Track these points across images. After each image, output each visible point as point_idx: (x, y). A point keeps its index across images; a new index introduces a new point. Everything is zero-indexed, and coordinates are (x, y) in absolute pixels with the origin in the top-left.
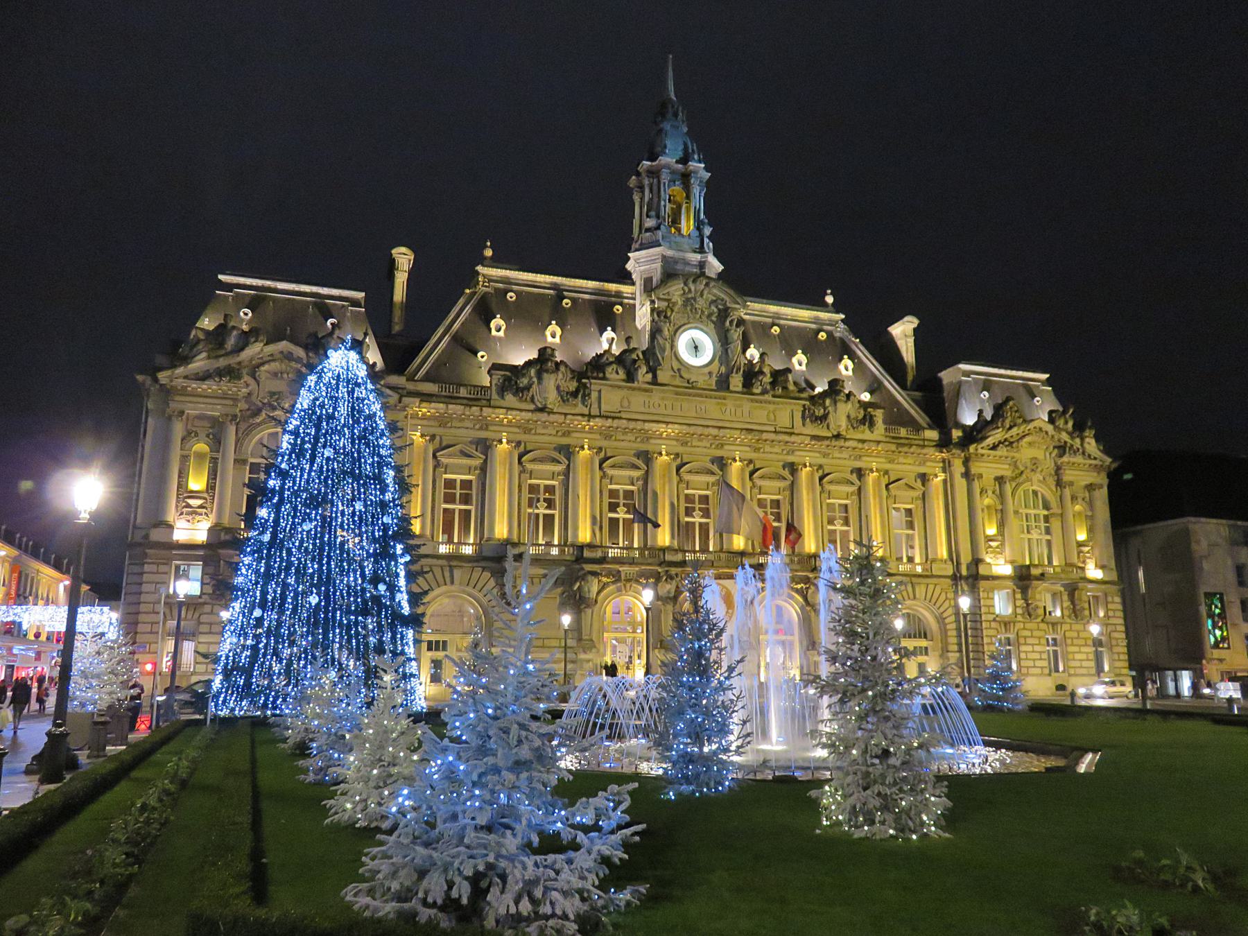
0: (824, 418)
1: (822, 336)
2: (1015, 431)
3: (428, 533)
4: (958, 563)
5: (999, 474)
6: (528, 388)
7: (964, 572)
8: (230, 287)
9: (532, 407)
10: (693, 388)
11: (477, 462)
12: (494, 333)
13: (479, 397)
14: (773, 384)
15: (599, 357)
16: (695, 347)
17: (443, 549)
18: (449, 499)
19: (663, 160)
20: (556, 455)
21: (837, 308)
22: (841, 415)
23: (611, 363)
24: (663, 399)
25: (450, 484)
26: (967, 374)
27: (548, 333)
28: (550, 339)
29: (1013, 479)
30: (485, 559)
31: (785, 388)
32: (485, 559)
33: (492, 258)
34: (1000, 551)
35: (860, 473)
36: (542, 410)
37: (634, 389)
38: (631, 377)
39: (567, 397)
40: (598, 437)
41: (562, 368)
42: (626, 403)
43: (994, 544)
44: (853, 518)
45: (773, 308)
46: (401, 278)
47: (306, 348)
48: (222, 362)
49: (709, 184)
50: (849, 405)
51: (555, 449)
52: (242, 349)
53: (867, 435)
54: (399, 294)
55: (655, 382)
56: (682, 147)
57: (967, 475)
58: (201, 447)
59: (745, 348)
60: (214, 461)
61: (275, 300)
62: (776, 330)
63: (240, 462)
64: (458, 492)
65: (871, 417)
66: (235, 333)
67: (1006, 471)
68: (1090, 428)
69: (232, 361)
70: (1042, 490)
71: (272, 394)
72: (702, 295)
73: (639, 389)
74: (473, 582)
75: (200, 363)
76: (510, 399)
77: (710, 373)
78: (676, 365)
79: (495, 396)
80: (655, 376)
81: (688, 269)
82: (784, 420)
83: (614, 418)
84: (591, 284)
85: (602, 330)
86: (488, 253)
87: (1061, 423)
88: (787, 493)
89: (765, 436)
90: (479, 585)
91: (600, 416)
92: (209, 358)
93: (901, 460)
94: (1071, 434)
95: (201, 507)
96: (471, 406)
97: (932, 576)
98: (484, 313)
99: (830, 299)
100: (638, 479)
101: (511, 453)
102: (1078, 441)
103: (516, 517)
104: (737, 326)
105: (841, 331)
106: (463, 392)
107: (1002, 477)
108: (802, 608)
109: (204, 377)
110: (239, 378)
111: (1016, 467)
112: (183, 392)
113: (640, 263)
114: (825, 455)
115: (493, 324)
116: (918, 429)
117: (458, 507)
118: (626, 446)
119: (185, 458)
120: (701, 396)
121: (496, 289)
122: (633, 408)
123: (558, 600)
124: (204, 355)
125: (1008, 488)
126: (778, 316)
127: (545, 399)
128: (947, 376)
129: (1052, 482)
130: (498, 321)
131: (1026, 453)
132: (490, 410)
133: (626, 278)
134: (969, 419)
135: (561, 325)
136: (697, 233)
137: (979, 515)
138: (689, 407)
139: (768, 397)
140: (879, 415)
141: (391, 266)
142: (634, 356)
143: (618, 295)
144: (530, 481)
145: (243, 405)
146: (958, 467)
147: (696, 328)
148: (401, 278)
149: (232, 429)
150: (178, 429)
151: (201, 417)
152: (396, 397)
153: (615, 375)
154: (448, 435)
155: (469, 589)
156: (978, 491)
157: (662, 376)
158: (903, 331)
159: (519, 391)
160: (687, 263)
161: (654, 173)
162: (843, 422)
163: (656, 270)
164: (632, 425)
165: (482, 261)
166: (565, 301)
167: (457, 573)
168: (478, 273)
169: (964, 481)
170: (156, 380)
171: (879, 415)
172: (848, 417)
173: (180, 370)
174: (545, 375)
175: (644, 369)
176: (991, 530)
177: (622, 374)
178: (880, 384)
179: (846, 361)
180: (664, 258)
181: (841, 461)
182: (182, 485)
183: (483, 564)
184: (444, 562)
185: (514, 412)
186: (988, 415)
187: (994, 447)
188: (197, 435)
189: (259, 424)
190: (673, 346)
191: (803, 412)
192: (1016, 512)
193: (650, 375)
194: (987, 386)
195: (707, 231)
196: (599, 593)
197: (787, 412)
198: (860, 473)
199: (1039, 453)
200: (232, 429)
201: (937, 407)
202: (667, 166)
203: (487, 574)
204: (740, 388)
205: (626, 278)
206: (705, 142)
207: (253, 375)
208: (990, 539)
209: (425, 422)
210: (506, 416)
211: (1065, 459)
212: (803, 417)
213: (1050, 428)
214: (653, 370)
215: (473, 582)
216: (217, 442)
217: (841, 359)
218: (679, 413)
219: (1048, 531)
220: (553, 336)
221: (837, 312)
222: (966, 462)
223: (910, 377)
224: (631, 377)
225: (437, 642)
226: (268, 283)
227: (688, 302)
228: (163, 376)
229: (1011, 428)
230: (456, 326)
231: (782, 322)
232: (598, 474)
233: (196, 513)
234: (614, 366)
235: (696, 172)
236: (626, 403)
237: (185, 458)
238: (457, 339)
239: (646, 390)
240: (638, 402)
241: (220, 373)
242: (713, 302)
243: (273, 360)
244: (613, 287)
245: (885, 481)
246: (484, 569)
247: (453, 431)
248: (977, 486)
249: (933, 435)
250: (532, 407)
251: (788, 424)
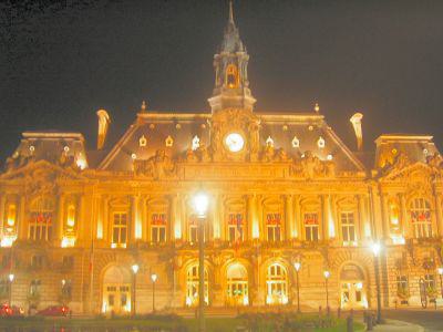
0: (301, 171)
1: (311, 128)
8: (27, 138)
13: (130, 176)
14: (274, 156)
15: (185, 152)
17: (114, 246)
18: (117, 223)
19: (223, 53)
21: (321, 112)
25: (117, 216)
26: (384, 141)
34: (399, 232)
38: (200, 160)
45: (285, 117)
50: (314, 164)
53: (326, 178)
55: (212, 161)
57: (379, 194)
58: (13, 207)
59: (266, 139)
63: (27, 211)
67: (401, 190)
75: (9, 173)
84: (192, 115)
86: (144, 107)
99: (317, 109)
103: (146, 230)
106: (121, 174)
109: (11, 178)
114: (301, 189)
126: (289, 120)
129: (430, 193)
131: (414, 181)
134: (383, 165)
140: (332, 168)
141: (97, 119)
143: (205, 119)
145: (27, 188)
146: (375, 191)
149: (23, 199)
156: (386, 201)
157: (217, 157)
160: (234, 101)
161: (220, 59)
162: (311, 172)
165: (140, 111)
171: (332, 168)
175: (206, 155)
179: (321, 140)
180: (223, 100)
186: (391, 161)
187: (394, 179)
196: (184, 263)
199: (421, 179)
206: (249, 41)
207: (31, 175)
211: (435, 181)
214: (211, 156)
216: (18, 204)
222: (379, 188)
226: (42, 134)
241: (17, 175)
244: (202, 115)
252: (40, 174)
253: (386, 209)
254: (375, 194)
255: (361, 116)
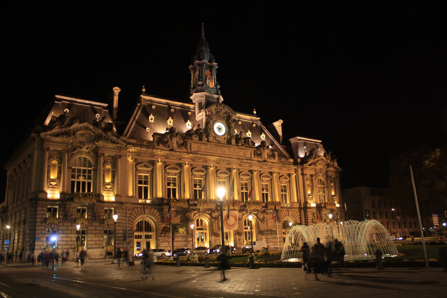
2: (316, 160)
3: (134, 195)
4: (301, 204)
5: (311, 173)
6: (167, 142)
7: (302, 206)
8: (60, 100)
9: (168, 149)
10: (220, 143)
11: (149, 169)
12: (150, 121)
13: (150, 145)
14: (245, 142)
16: (220, 129)
18: (140, 182)
20: (176, 166)
21: (257, 115)
22: (266, 153)
23: (194, 134)
24: (211, 147)
26: (299, 140)
27: (168, 122)
28: (169, 124)
29: (315, 175)
30: (156, 205)
31: (248, 144)
32: (156, 205)
33: (145, 92)
35: (271, 173)
36: (172, 150)
37: (201, 143)
38: (201, 139)
39: (180, 146)
40: (190, 160)
41: (179, 136)
42: (199, 149)
43: (310, 197)
44: (269, 188)
46: (116, 99)
47: (93, 125)
48: (64, 130)
49: (217, 70)
51: (176, 164)
52: (71, 125)
54: (115, 104)
55: (208, 141)
56: (209, 57)
57: (302, 174)
58: (55, 162)
60: (60, 168)
61: (76, 106)
62: (240, 123)
63: (69, 168)
64: (143, 180)
65: (274, 154)
66: (68, 119)
68: (336, 158)
69: (67, 129)
70: (323, 179)
71: (81, 142)
72: (221, 110)
73: (203, 143)
74: (151, 214)
76: (161, 146)
77: (225, 138)
78: (214, 135)
79: (156, 145)
80: (208, 139)
81: (213, 100)
82: (248, 155)
83: (196, 154)
85: (186, 121)
87: (327, 157)
88: (250, 180)
89: (244, 161)
90: (154, 214)
91: (191, 153)
92: (59, 128)
93: (283, 169)
94: (330, 161)
95: (56, 185)
96: (149, 148)
97: (293, 208)
98: (146, 112)
99: (255, 112)
100: (203, 176)
101: (162, 166)
102: (332, 163)
104: (233, 122)
105: (259, 123)
107: (312, 175)
108: (256, 220)
109: (57, 135)
110: (70, 136)
111: (316, 171)
112: (49, 141)
113: (196, 97)
114: (261, 168)
115: (150, 118)
116: (287, 159)
117: (143, 186)
118: (199, 164)
119: (49, 166)
120: (223, 146)
121: (148, 104)
122: (202, 150)
123: (180, 219)
124: (58, 127)
125: (314, 178)
127: (173, 146)
128: (292, 140)
129: (325, 176)
130: (151, 116)
131: (319, 167)
132: (156, 150)
133: (190, 102)
134: (302, 155)
135: (172, 118)
136: (215, 88)
137: (307, 187)
138: (219, 150)
139: (243, 147)
140: (276, 153)
141: (112, 94)
142: (201, 131)
143: (189, 108)
144: (168, 176)
145: (70, 147)
146: (300, 172)
147: (220, 122)
148: (116, 99)
150: (47, 154)
151: (55, 150)
152: (125, 144)
153: (195, 138)
154: (140, 159)
155: (150, 216)
157: (211, 139)
158: (278, 125)
159: (165, 143)
160: (213, 98)
161: (201, 65)
162: (266, 156)
163: (203, 100)
164: (202, 156)
165: (141, 93)
166: (172, 109)
167: (146, 210)
168: (141, 98)
169: (301, 176)
170: (39, 136)
171: (276, 153)
172: (268, 154)
173: (49, 132)
174: (173, 138)
175: (204, 136)
176: (309, 192)
177: (197, 138)
178: (274, 143)
181: (266, 170)
182: (49, 177)
183: (155, 207)
184: (142, 206)
185: (164, 151)
187: (310, 165)
188: (53, 157)
189: (76, 154)
190: (213, 128)
191: (254, 152)
192: (316, 186)
193: (206, 139)
194: (305, 144)
195: (219, 87)
197: (249, 153)
198: (271, 173)
200: (67, 155)
201: (292, 152)
202: (205, 63)
203: (156, 211)
204: (234, 144)
205: (190, 102)
206: (217, 55)
208: (309, 195)
209: (132, 154)
210: (160, 152)
211: (329, 169)
212: (254, 154)
213: (324, 158)
214: (207, 137)
215: (151, 214)
216: (61, 161)
217: (261, 134)
218: (216, 152)
219: (324, 192)
220: (170, 123)
221: (258, 117)
222: (302, 170)
223: (281, 141)
224: (201, 139)
225: (138, 236)
226: (74, 99)
227: (217, 113)
228: (42, 134)
229: (315, 159)
230: (137, 117)
231: (241, 120)
232: (191, 174)
233: (54, 187)
234: (195, 135)
235: (214, 66)
236: (199, 149)
237: (49, 166)
238: (137, 122)
239: (205, 144)
240: (203, 147)
242: (225, 113)
243: (82, 130)
244: (187, 105)
245: (278, 176)
246: (155, 208)
247: (142, 157)
248: (305, 177)
249: (291, 160)
250: (168, 149)
251: (250, 157)
252: (82, 135)
253: (306, 185)
254: (300, 174)
255: (282, 121)
